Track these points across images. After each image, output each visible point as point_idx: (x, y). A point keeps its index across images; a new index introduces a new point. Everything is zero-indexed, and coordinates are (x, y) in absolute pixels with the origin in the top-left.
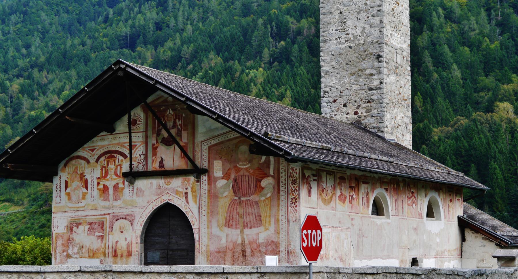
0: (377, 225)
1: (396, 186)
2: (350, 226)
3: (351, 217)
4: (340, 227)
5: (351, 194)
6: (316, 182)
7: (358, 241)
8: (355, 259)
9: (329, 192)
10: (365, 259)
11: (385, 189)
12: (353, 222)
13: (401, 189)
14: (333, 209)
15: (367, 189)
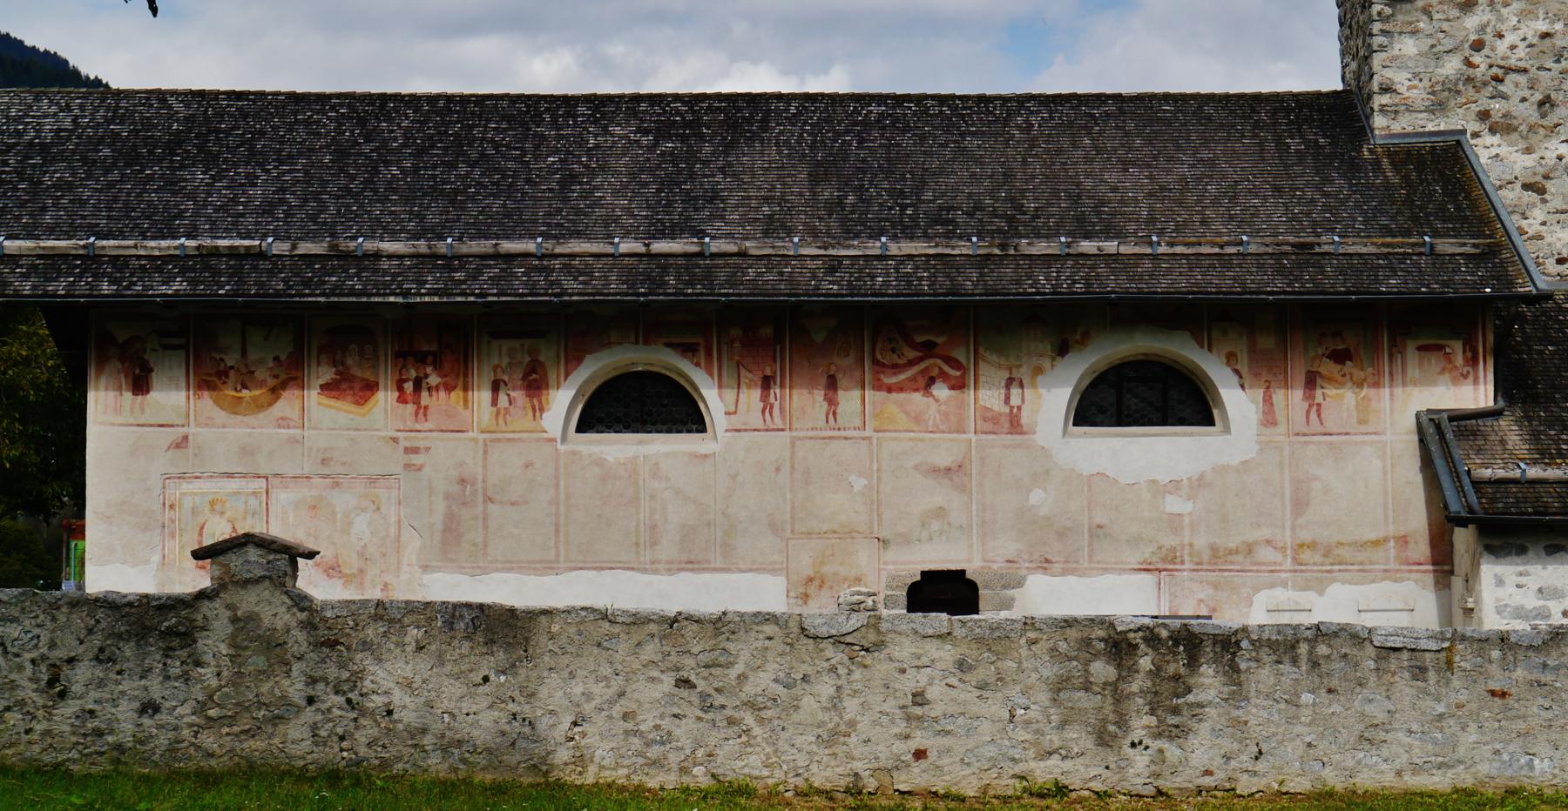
0: (599, 462)
1: (767, 331)
2: (397, 469)
3: (403, 444)
4: (325, 477)
5: (413, 374)
6: (182, 353)
7: (450, 517)
8: (426, 568)
9: (261, 374)
10: (497, 570)
11: (667, 345)
12: (417, 459)
13: (819, 337)
14: (283, 422)
15: (533, 352)
